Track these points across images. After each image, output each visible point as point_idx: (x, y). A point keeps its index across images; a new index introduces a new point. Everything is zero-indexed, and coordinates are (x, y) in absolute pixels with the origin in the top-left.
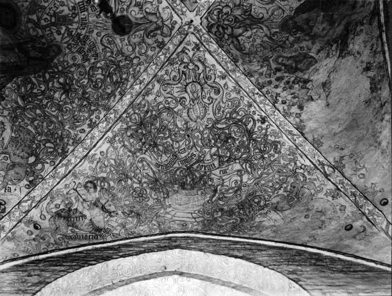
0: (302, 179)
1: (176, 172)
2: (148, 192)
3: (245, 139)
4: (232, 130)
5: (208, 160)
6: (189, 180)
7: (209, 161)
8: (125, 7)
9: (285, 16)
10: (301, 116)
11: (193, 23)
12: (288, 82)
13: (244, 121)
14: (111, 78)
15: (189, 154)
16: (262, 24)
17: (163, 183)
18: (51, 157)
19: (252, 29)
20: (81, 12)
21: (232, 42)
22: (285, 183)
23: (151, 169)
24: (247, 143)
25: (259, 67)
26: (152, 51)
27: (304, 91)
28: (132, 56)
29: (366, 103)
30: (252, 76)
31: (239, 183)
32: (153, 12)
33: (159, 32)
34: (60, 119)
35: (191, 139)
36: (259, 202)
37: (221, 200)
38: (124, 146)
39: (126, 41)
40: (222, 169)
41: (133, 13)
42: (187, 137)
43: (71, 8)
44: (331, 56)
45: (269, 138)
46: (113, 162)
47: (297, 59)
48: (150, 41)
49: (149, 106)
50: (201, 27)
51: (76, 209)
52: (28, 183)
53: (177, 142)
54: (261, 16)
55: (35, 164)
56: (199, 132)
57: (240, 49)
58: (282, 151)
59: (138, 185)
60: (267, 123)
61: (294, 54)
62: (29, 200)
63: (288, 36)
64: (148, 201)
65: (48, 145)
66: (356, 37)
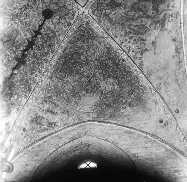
0: (142, 91)
1: (83, 83)
2: (71, 98)
3: (115, 67)
4: (109, 61)
5: (98, 76)
6: (89, 87)
7: (99, 77)
8: (48, 5)
9: (133, 2)
10: (141, 59)
11: (85, 13)
12: (135, 40)
13: (114, 58)
14: (46, 43)
15: (88, 73)
16: (121, 6)
17: (77, 91)
18: (24, 93)
19: (115, 10)
20: (25, 10)
21: (106, 18)
22: (134, 92)
23: (71, 84)
24: (116, 69)
25: (120, 31)
26: (64, 27)
27: (143, 45)
28: (55, 31)
29: (173, 57)
30: (117, 37)
31: (113, 89)
32: (63, 6)
33: (67, 17)
34: (24, 71)
35: (89, 65)
36: (122, 100)
37: (104, 98)
38: (57, 78)
39: (51, 22)
40: (105, 81)
41: (52, 7)
42: (87, 64)
43: (19, 9)
44: (157, 29)
45: (126, 69)
46: (53, 87)
47: (140, 27)
48: (63, 21)
49: (66, 55)
50: (89, 15)
51: (40, 116)
52: (17, 110)
53: (82, 67)
54: (120, 2)
55: (17, 99)
56: (93, 61)
57: (110, 21)
58: (133, 76)
59: (66, 96)
60: (125, 62)
61: (138, 24)
62: (18, 121)
63: (135, 14)
64: (71, 103)
65: (22, 87)
66: (169, 23)
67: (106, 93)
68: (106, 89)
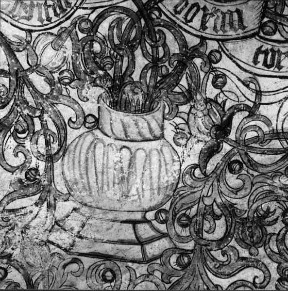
1: (95, 26)
6: (141, 62)
37: (232, 171)
67: (251, 134)
68: (257, 105)
